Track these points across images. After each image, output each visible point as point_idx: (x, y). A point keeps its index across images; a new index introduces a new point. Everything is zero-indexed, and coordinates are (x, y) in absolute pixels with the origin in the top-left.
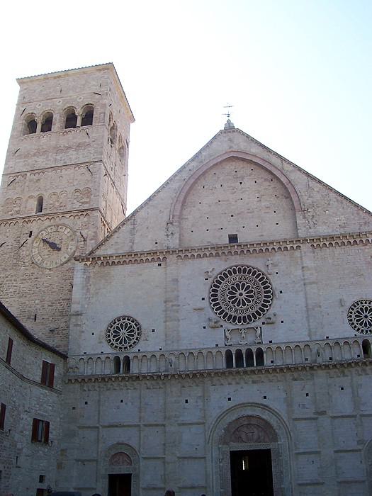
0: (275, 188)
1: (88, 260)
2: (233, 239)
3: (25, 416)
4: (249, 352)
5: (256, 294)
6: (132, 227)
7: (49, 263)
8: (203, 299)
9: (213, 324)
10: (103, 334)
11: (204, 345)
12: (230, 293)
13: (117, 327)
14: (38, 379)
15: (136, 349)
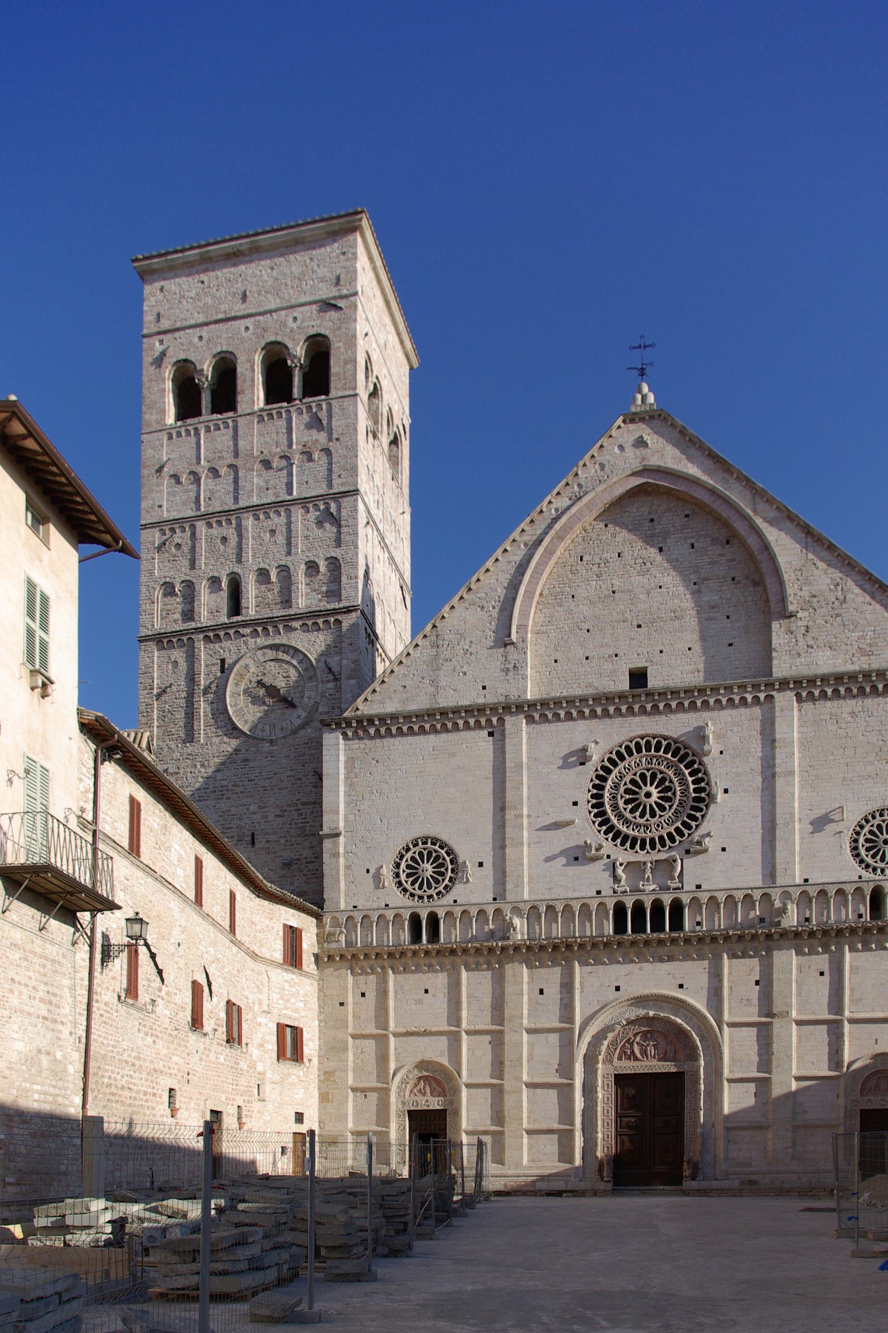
0: (731, 560)
1: (349, 724)
2: (638, 678)
3: (262, 1020)
4: (658, 906)
5: (678, 793)
6: (433, 652)
7: (267, 728)
8: (575, 804)
9: (593, 852)
10: (387, 873)
11: (575, 891)
12: (627, 791)
13: (413, 859)
14: (279, 956)
15: (448, 899)
